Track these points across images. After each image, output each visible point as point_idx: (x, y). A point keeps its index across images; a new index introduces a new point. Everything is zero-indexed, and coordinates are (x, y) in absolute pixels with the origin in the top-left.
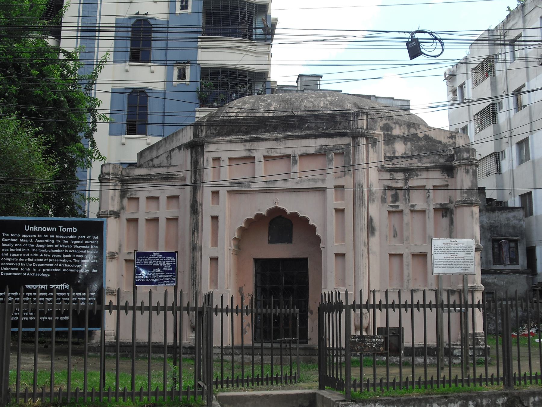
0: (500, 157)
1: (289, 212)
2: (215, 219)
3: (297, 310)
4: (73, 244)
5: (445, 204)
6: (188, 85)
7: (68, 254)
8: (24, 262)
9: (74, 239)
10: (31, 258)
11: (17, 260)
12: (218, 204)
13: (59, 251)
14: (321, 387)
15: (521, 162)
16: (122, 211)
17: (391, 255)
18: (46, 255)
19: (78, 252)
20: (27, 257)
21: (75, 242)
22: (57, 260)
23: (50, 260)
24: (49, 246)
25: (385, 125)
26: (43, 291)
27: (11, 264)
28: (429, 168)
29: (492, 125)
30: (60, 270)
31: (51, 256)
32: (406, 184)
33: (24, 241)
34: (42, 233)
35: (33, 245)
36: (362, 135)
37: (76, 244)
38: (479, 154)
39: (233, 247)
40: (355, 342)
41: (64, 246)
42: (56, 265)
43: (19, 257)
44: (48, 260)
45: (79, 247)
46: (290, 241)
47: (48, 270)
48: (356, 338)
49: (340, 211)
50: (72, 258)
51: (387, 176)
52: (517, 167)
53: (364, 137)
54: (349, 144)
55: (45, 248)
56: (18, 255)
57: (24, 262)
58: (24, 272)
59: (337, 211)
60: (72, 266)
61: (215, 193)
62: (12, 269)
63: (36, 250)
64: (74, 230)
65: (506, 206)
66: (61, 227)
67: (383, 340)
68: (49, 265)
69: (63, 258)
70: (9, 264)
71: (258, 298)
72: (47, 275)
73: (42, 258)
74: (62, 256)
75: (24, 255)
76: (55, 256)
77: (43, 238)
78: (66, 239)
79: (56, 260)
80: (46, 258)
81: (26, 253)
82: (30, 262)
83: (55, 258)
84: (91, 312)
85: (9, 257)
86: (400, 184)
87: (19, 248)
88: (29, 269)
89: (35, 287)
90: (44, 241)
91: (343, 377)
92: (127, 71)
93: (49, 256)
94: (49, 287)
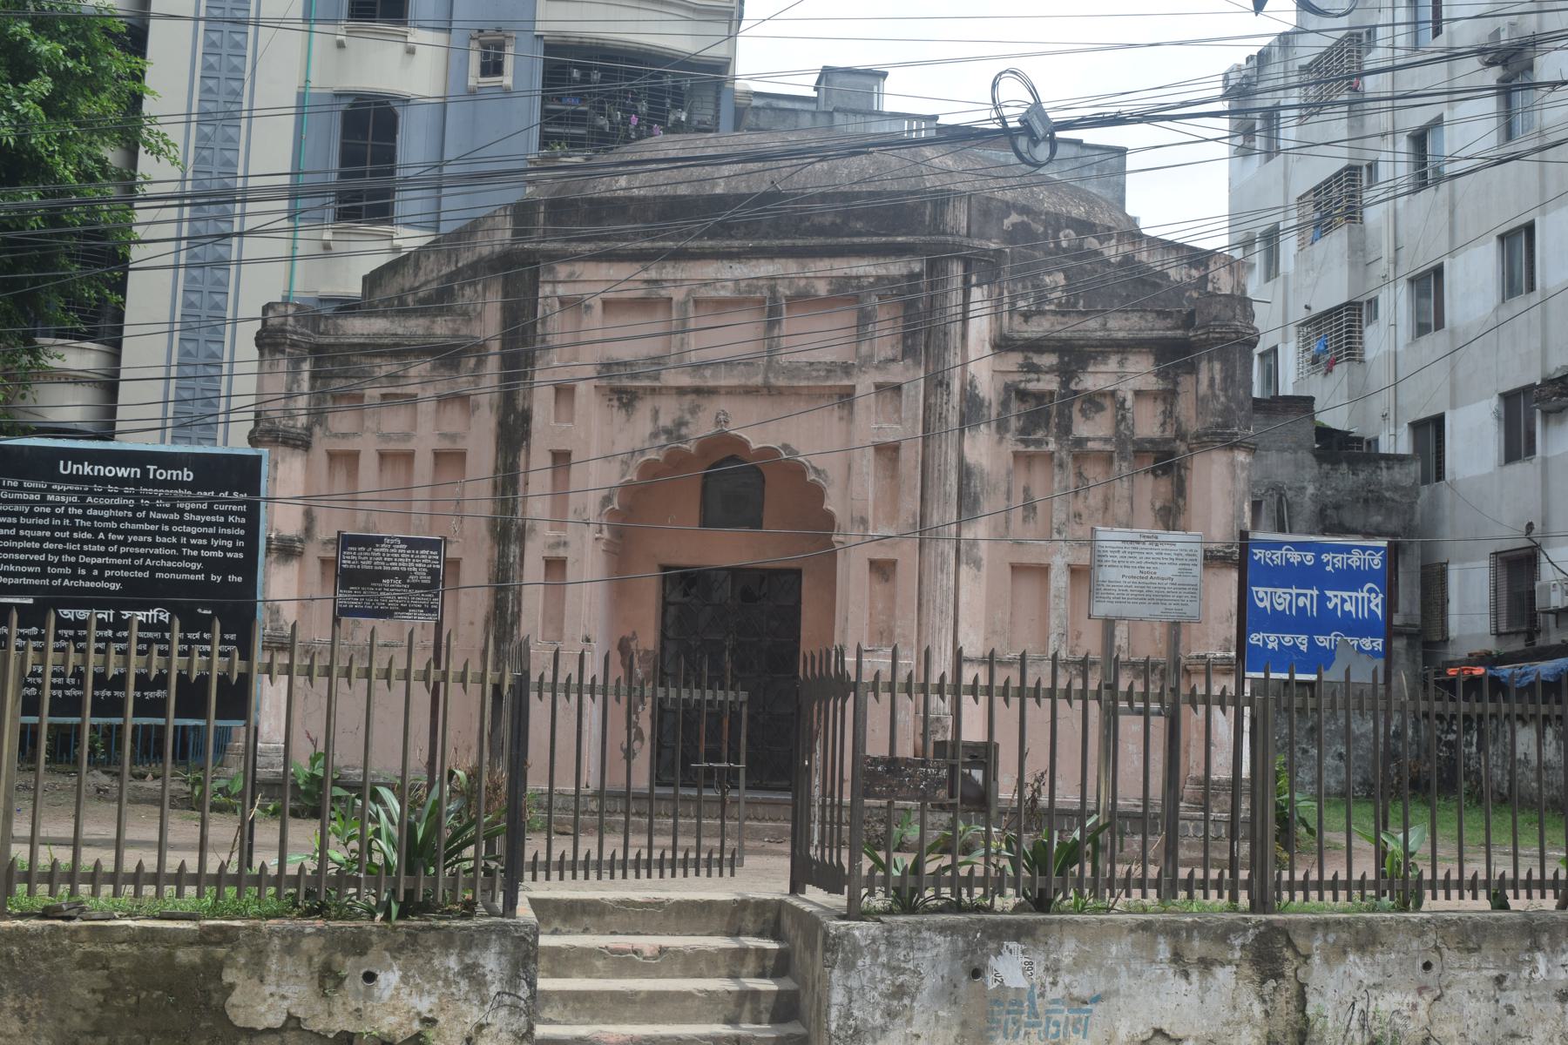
0: (1364, 317)
1: (754, 445)
2: (561, 459)
3: (743, 696)
4: (181, 512)
5: (1167, 441)
6: (507, 91)
7: (169, 534)
8: (55, 552)
9: (184, 500)
10: (75, 541)
11: (37, 545)
12: (571, 420)
13: (146, 527)
14: (796, 888)
15: (1422, 329)
16: (317, 430)
17: (1016, 569)
18: (111, 536)
19: (194, 530)
20: (63, 541)
21: (188, 506)
22: (142, 550)
23: (123, 550)
24: (121, 514)
25: (1014, 225)
26: (102, 625)
27: (22, 557)
28: (1125, 347)
29: (1346, 228)
30: (147, 574)
31: (126, 539)
32: (1065, 384)
33: (58, 499)
34: (104, 480)
35: (80, 512)
36: (955, 252)
37: (192, 511)
38: (1306, 307)
39: (606, 534)
40: (874, 772)
41: (159, 516)
42: (139, 562)
43: (42, 540)
44: (118, 549)
45: (198, 518)
46: (756, 523)
47: (118, 573)
48: (876, 766)
49: (888, 452)
50: (178, 546)
51: (1013, 360)
52: (1408, 345)
53: (958, 258)
54: (919, 276)
55: (110, 519)
56: (40, 534)
57: (55, 552)
58: (56, 576)
59: (880, 448)
60: (180, 564)
61: (564, 392)
62: (23, 569)
63: (88, 524)
64: (187, 475)
65: (1373, 451)
66: (152, 468)
67: (944, 773)
68: (119, 561)
69: (154, 545)
70: (17, 556)
71: (666, 670)
72: (115, 586)
73: (101, 542)
74: (154, 539)
75: (58, 534)
76: (135, 538)
77: (105, 494)
78: (165, 499)
79: (137, 550)
80: (113, 543)
81: (62, 528)
82: (71, 553)
83: (135, 544)
84: (223, 680)
85: (17, 538)
86: (1050, 383)
87: (42, 515)
88: (68, 571)
89: (83, 614)
90: (108, 502)
91: (845, 862)
92: (341, 45)
93: (121, 538)
94: (117, 616)
